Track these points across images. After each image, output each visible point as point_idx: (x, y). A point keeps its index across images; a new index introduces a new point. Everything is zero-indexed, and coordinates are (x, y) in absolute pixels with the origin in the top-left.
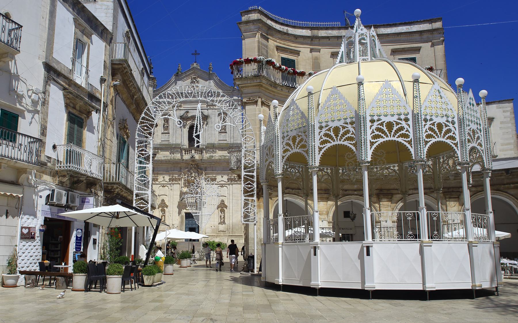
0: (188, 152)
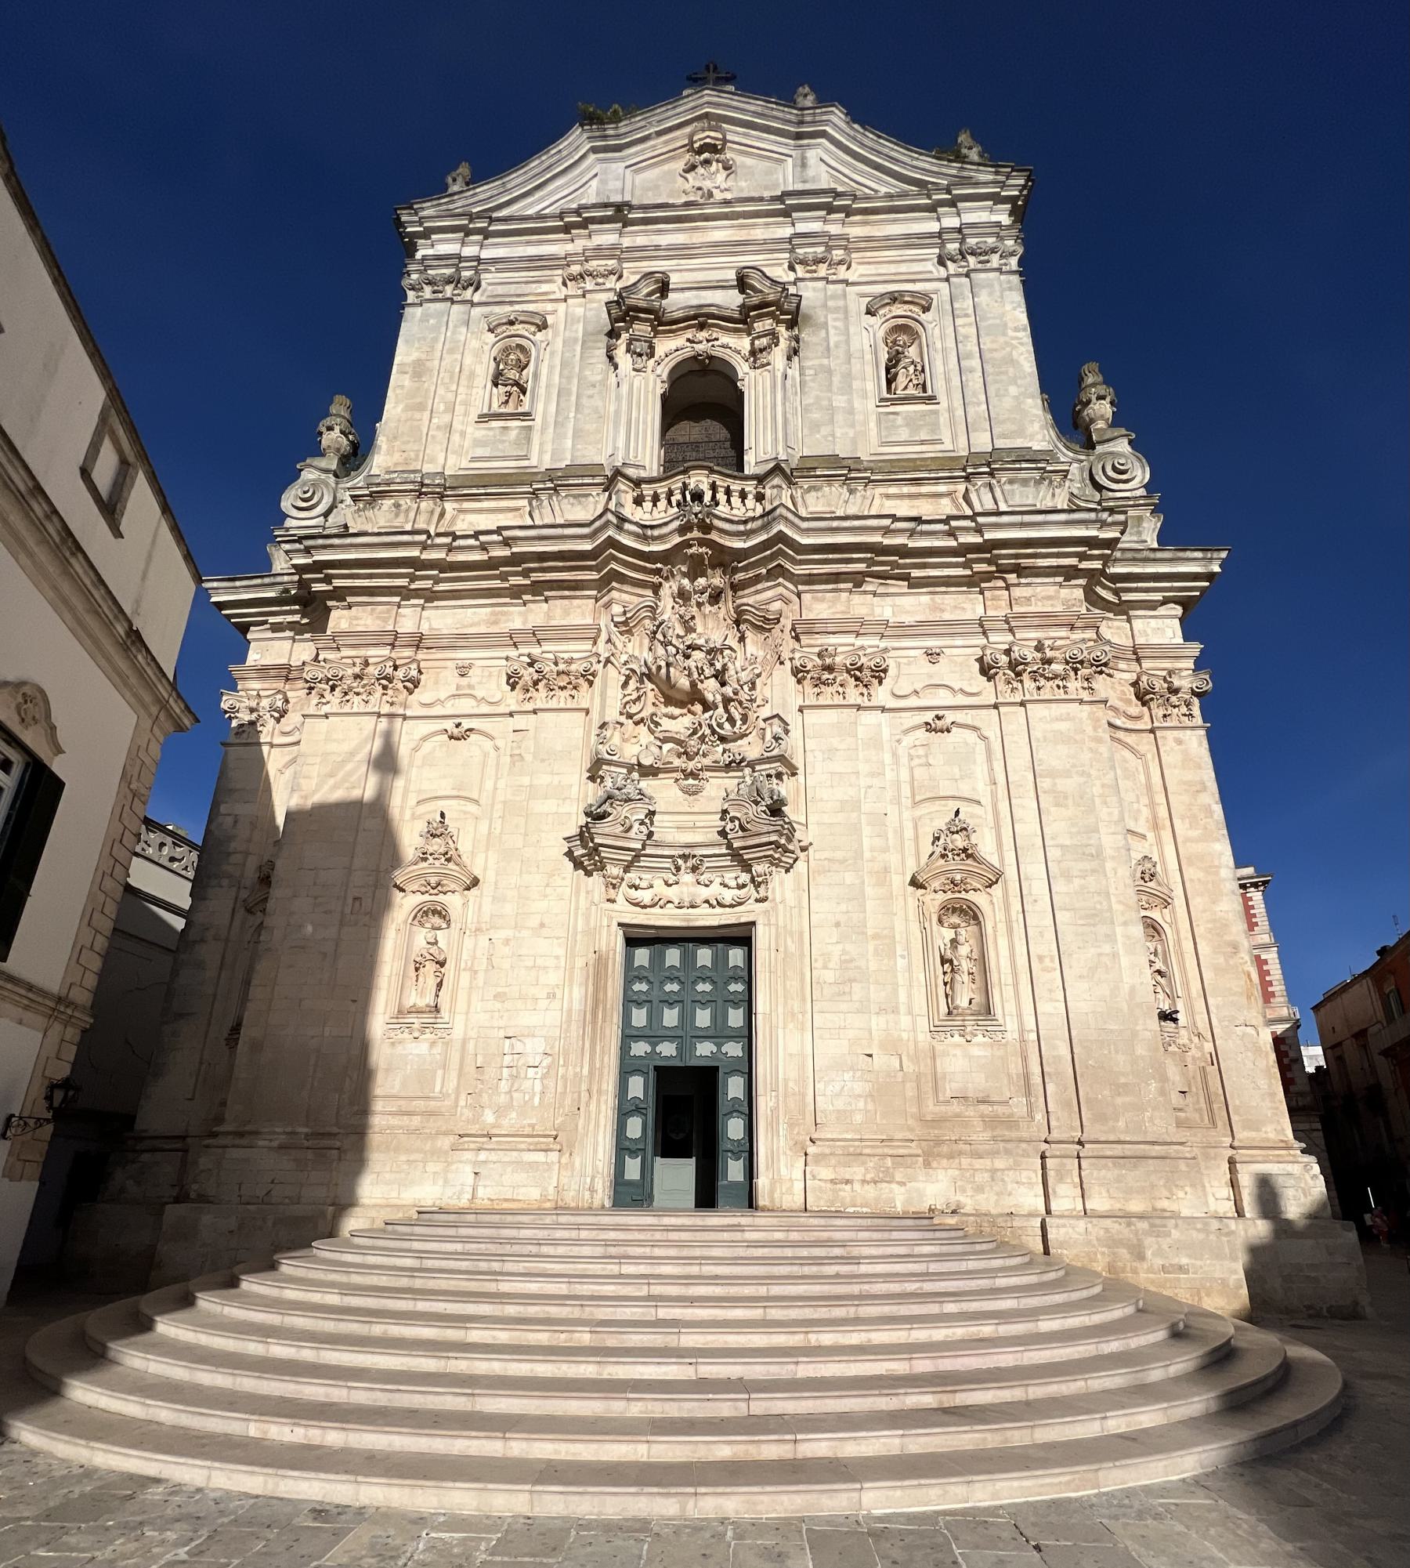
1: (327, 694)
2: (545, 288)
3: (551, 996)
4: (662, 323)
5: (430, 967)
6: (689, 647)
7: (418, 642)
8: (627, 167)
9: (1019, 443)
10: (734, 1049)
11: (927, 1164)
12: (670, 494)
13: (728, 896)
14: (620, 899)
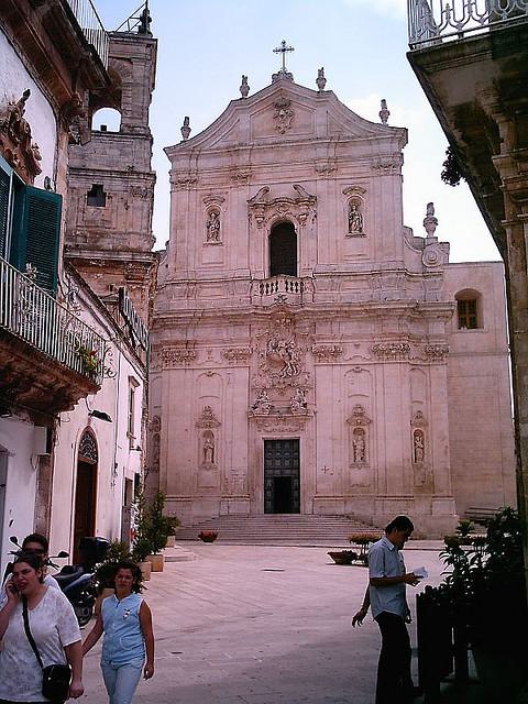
0: (270, 289)
10: (295, 472)
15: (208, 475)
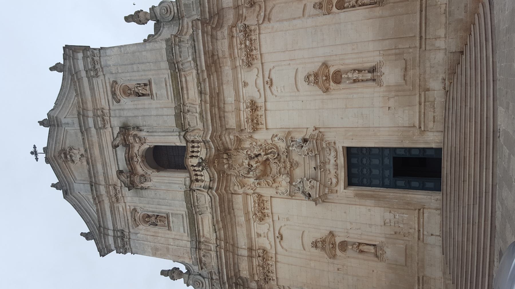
1: (269, 278)
2: (121, 209)
3: (369, 210)
4: (132, 172)
5: (361, 247)
6: (249, 166)
7: (250, 249)
8: (75, 183)
9: (164, 52)
11: (428, 90)
12: (195, 170)
13: (333, 154)
14: (336, 188)
15: (389, 252)
